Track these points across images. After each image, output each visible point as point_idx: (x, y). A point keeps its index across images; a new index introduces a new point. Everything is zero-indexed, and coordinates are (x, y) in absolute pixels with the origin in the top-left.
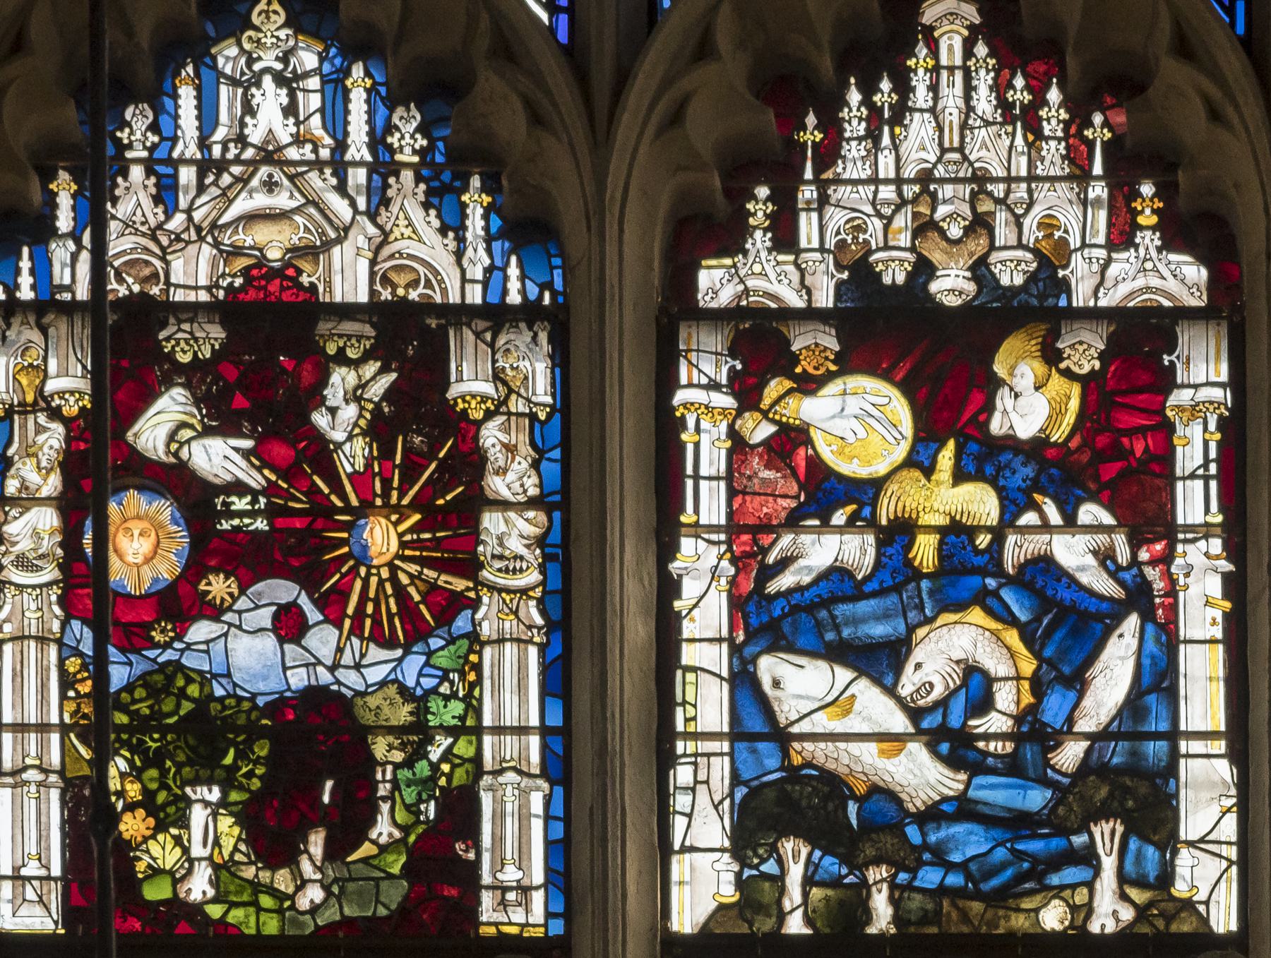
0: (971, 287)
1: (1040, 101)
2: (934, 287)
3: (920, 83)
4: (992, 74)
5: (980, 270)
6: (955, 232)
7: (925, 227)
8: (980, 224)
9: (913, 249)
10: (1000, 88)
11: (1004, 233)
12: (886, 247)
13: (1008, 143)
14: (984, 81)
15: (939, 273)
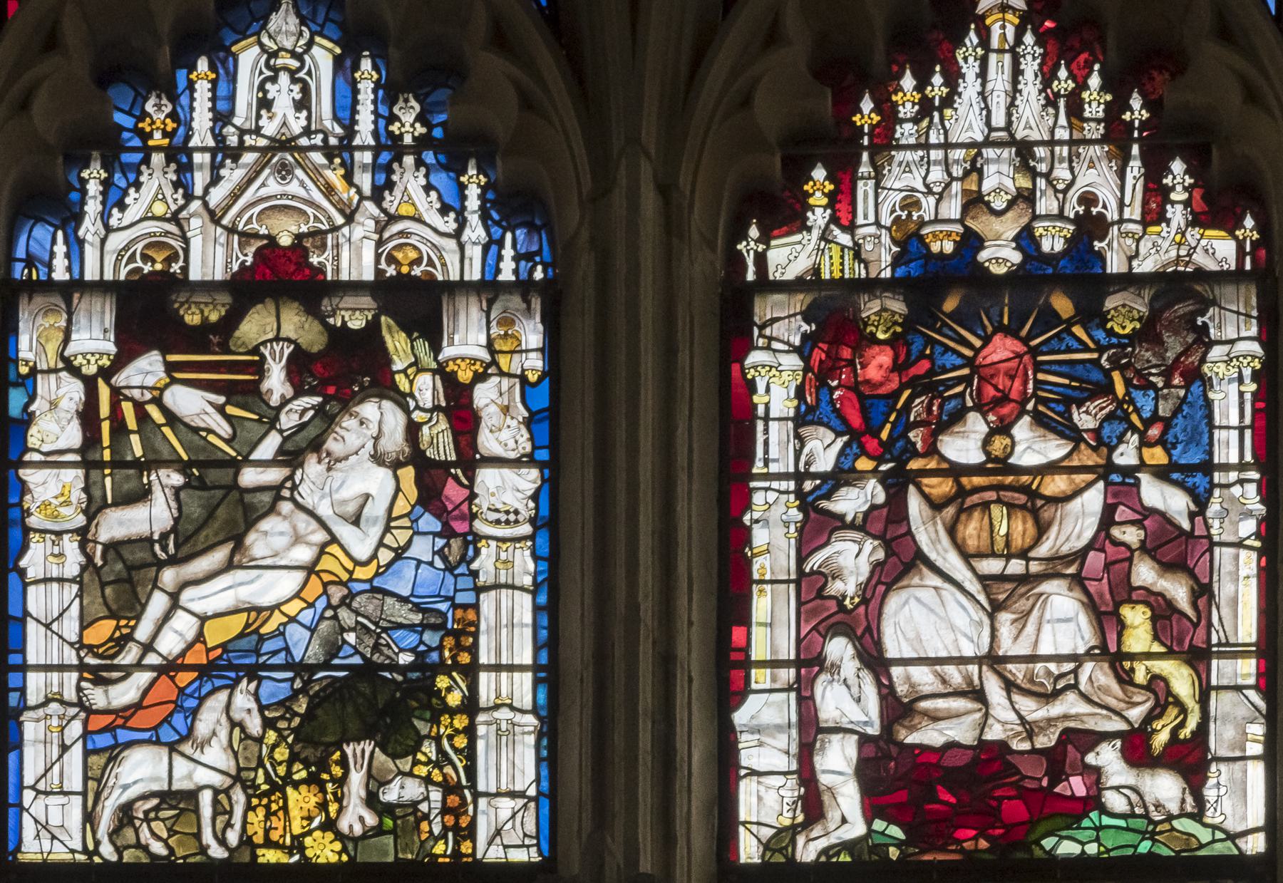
0: (1016, 257)
1: (1082, 85)
2: (983, 256)
3: (970, 70)
4: (1038, 61)
5: (1025, 239)
6: (999, 204)
7: (974, 202)
8: (1026, 198)
9: (961, 221)
10: (1047, 76)
11: (1046, 204)
12: (936, 221)
13: (1051, 122)
14: (1030, 67)
15: (987, 244)
